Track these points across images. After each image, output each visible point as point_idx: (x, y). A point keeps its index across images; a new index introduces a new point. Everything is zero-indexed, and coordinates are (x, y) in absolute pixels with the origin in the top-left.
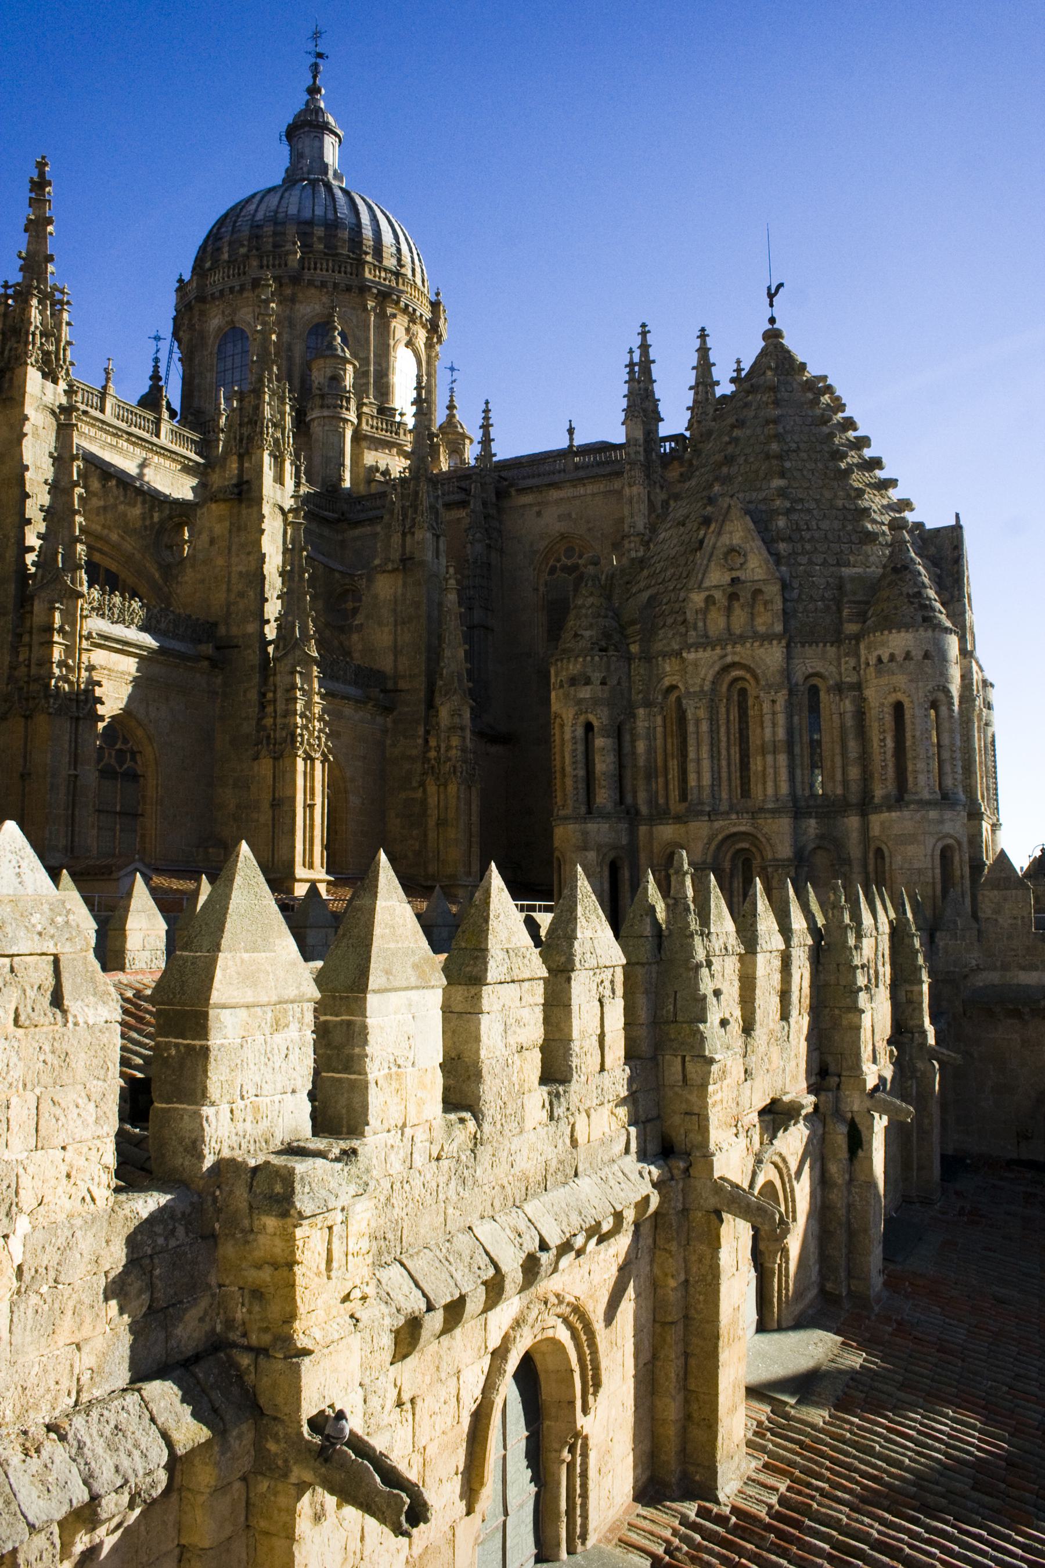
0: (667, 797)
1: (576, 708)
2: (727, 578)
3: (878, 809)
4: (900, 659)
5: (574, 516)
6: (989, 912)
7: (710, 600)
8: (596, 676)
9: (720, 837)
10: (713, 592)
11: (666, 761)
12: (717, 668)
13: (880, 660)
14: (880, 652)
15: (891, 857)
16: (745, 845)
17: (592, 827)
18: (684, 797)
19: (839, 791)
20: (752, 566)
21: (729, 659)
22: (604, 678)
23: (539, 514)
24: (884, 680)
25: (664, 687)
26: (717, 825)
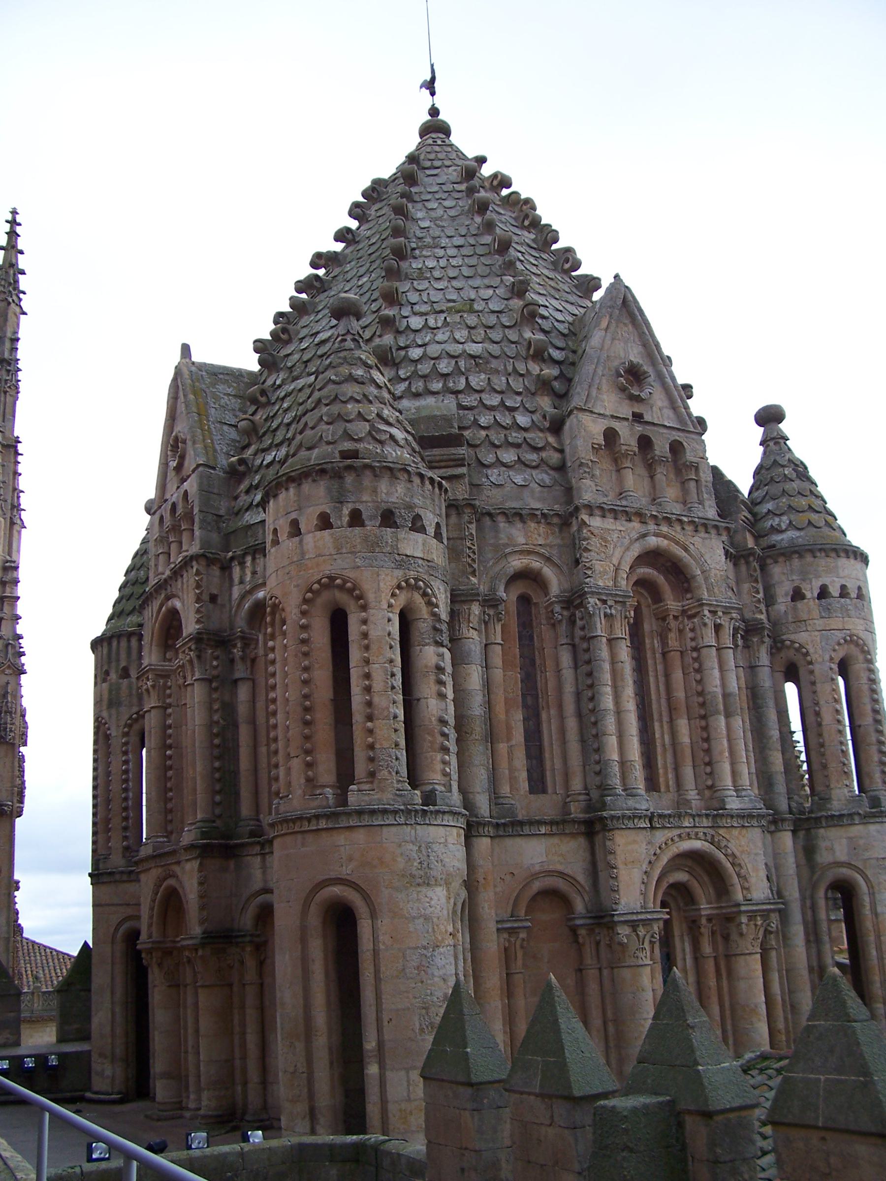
0: (513, 780)
1: (399, 573)
2: (626, 411)
3: (838, 820)
4: (853, 595)
7: (610, 435)
9: (664, 860)
10: (616, 425)
11: (507, 712)
12: (636, 550)
13: (823, 593)
14: (826, 580)
15: (872, 895)
16: (681, 876)
18: (538, 784)
20: (659, 404)
21: (653, 541)
24: (836, 623)
25: (511, 571)
26: (660, 836)
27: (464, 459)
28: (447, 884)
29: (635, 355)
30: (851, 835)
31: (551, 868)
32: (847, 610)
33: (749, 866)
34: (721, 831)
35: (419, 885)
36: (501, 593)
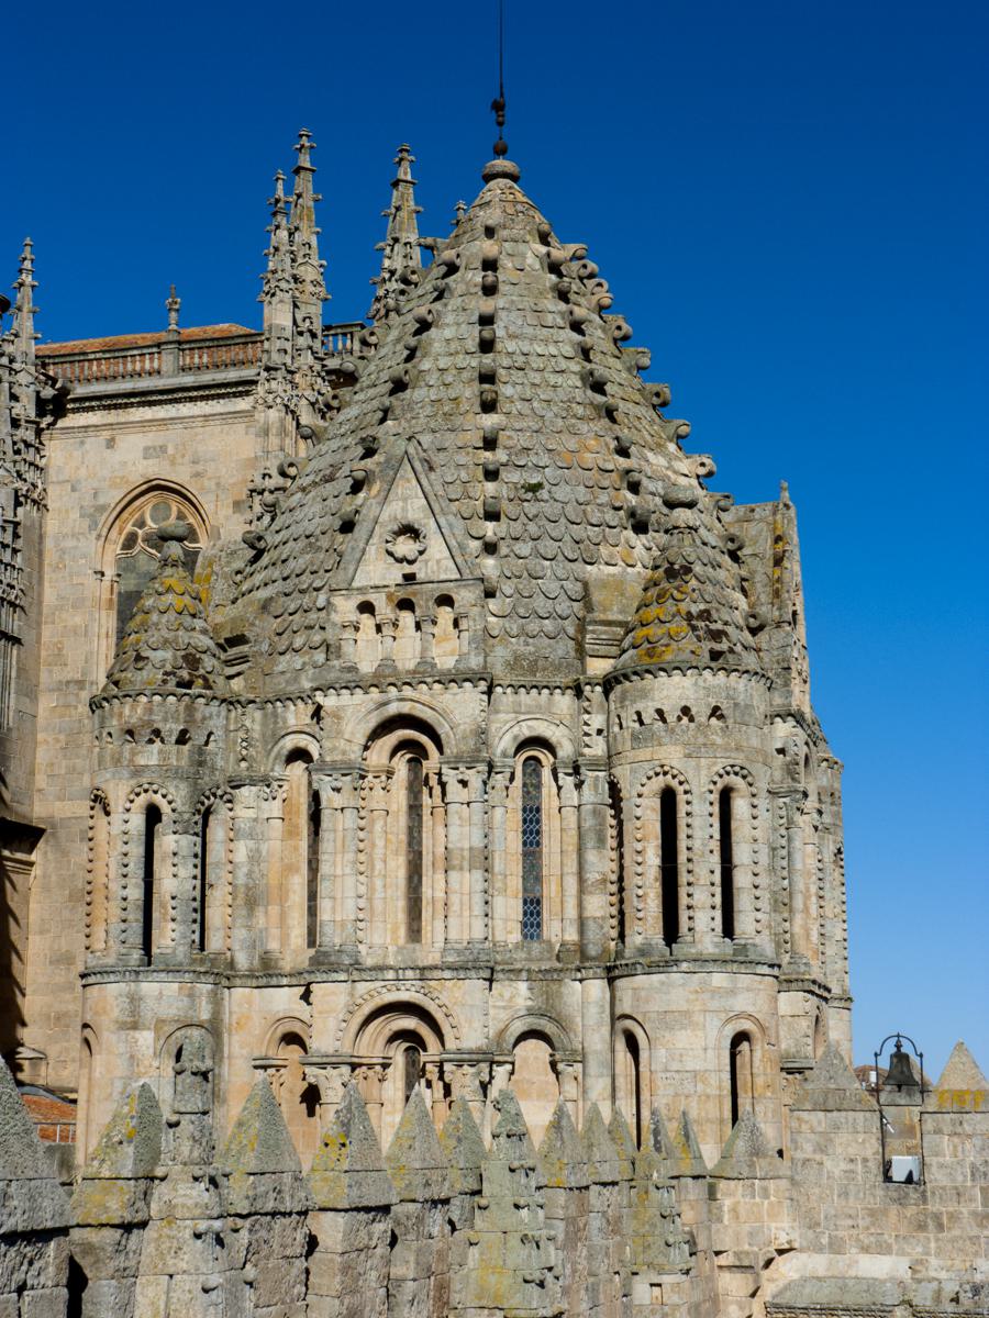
0: (284, 939)
1: (133, 782)
2: (396, 574)
5: (171, 451)
6: (808, 1147)
8: (172, 728)
10: (372, 597)
14: (639, 706)
16: (409, 1023)
17: (149, 988)
19: (572, 936)
20: (438, 556)
21: (394, 709)
22: (184, 732)
23: (111, 443)
24: (644, 754)
26: (362, 987)
27: (246, 656)
28: (157, 1030)
29: (415, 511)
30: (636, 986)
31: (288, 1015)
32: (660, 738)
33: (462, 1018)
34: (432, 983)
35: (128, 1029)
36: (278, 771)
